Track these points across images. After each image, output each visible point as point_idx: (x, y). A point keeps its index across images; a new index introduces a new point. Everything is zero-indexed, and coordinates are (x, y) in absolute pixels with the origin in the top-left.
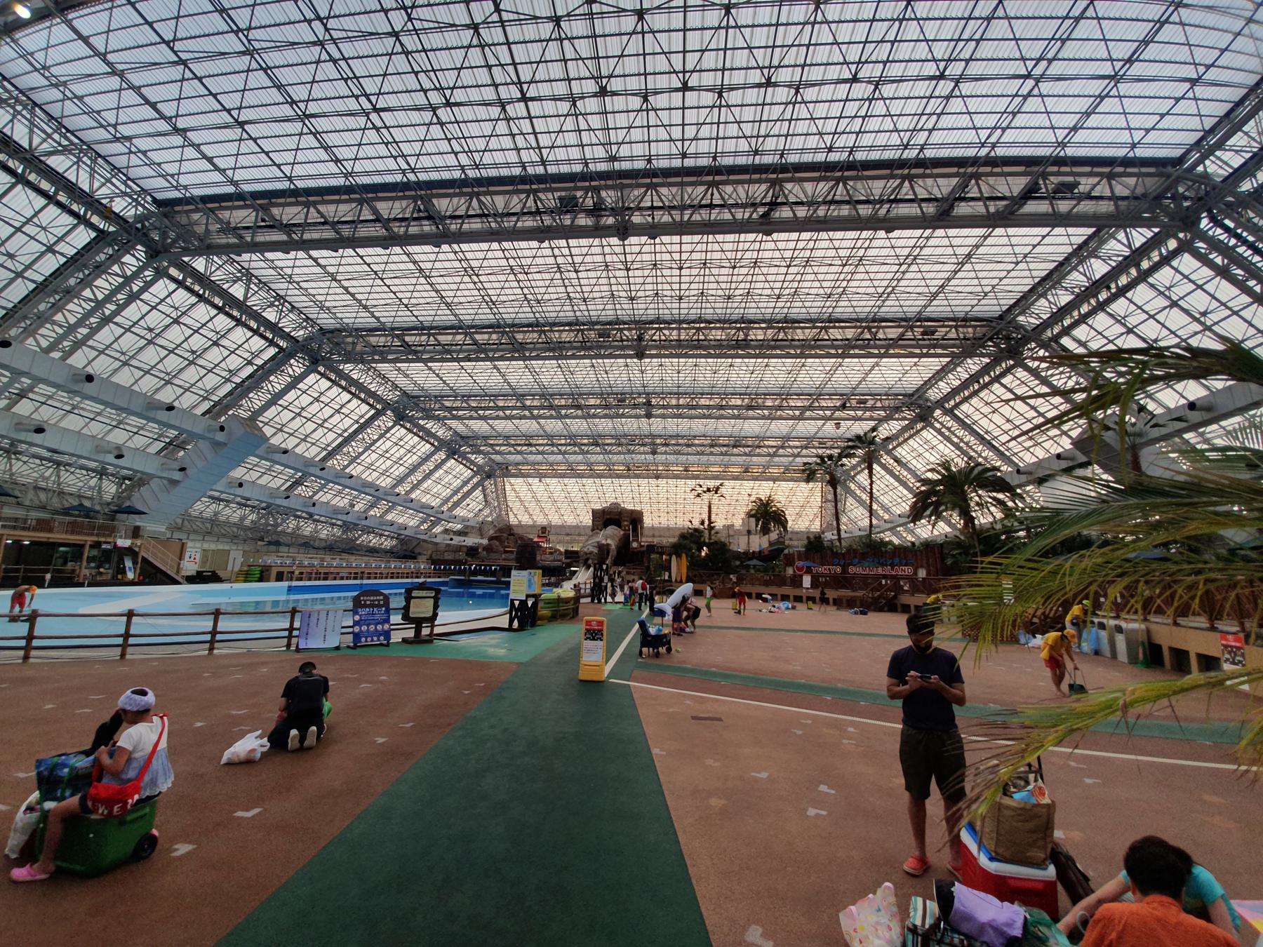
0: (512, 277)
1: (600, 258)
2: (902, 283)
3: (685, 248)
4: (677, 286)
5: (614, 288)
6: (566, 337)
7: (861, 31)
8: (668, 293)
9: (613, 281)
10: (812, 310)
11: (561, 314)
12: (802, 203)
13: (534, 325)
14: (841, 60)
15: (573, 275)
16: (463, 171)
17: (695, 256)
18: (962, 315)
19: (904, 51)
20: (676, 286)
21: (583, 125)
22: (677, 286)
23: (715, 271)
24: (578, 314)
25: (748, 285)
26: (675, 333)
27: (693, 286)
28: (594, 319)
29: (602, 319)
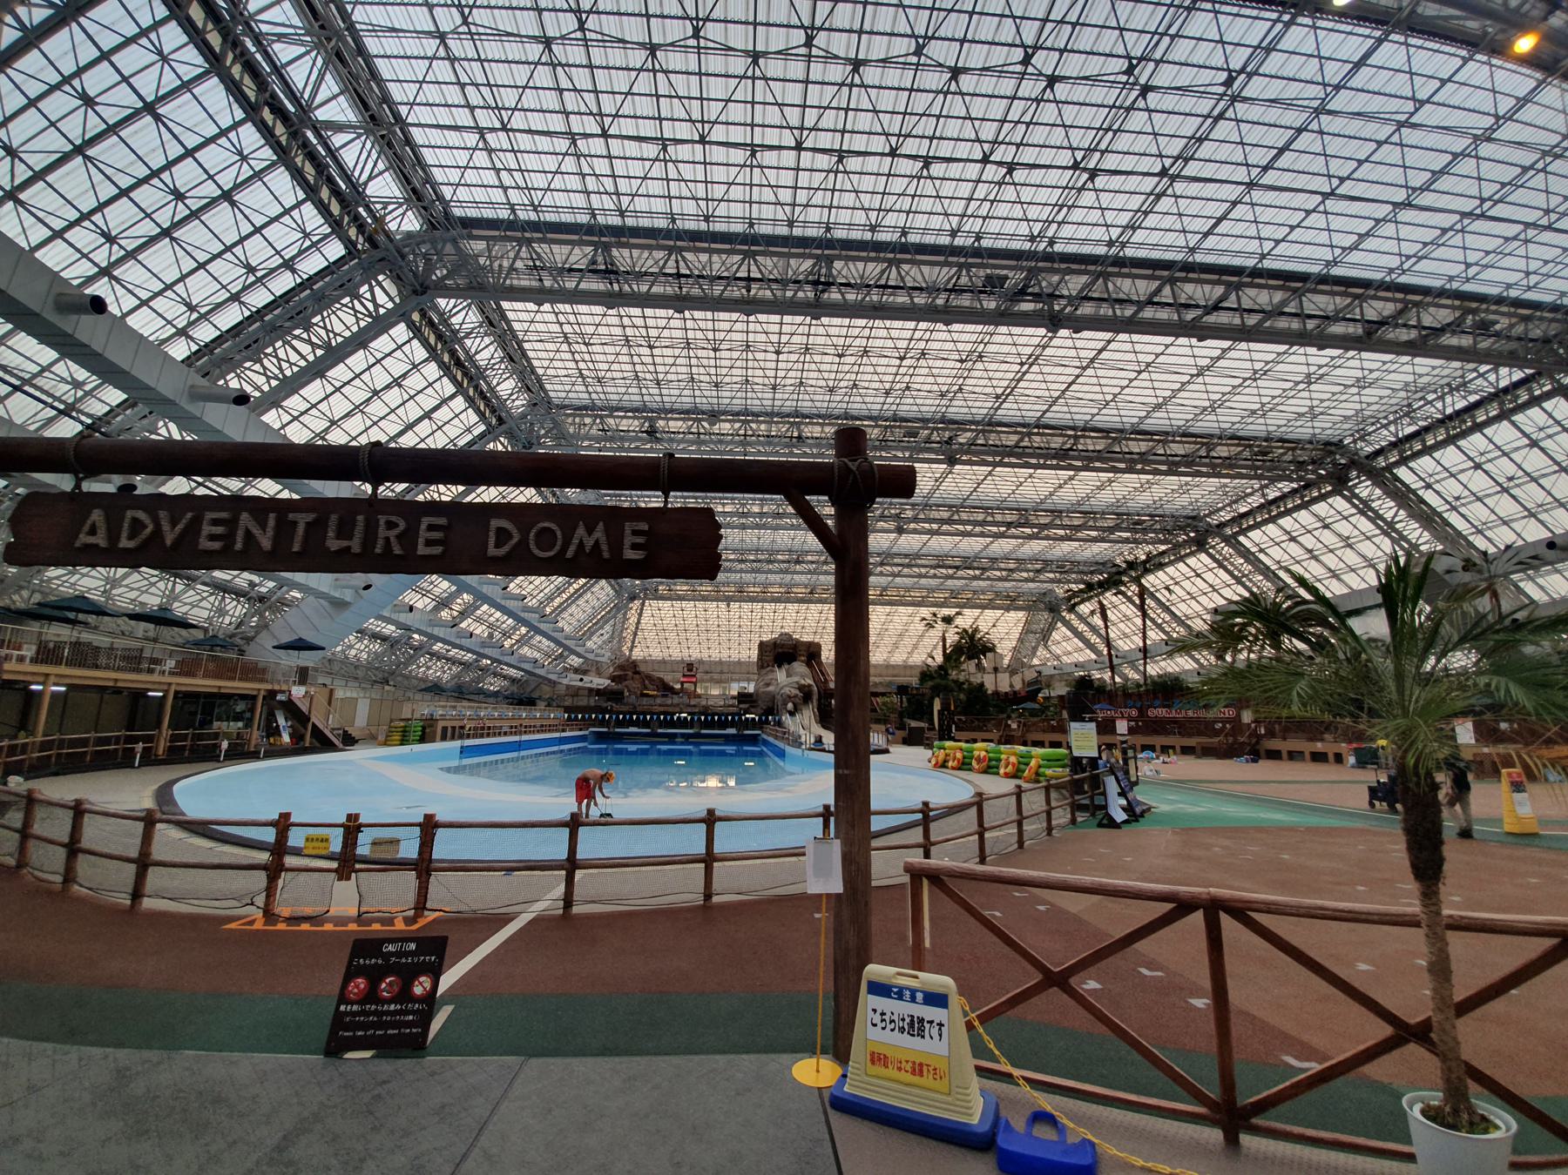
0: (565, 347)
1: (679, 334)
2: (1022, 384)
3: (786, 329)
4: (772, 373)
5: (695, 370)
6: (624, 425)
7: (997, 109)
8: (760, 380)
9: (694, 361)
10: (923, 409)
11: (626, 397)
12: (921, 289)
13: (589, 408)
14: (973, 136)
15: (647, 351)
16: (513, 211)
17: (795, 339)
18: (1081, 424)
19: (1038, 135)
20: (771, 373)
21: (673, 174)
22: (772, 373)
23: (817, 358)
24: (646, 398)
25: (853, 377)
26: (763, 427)
27: (791, 374)
28: (668, 406)
29: (676, 406)
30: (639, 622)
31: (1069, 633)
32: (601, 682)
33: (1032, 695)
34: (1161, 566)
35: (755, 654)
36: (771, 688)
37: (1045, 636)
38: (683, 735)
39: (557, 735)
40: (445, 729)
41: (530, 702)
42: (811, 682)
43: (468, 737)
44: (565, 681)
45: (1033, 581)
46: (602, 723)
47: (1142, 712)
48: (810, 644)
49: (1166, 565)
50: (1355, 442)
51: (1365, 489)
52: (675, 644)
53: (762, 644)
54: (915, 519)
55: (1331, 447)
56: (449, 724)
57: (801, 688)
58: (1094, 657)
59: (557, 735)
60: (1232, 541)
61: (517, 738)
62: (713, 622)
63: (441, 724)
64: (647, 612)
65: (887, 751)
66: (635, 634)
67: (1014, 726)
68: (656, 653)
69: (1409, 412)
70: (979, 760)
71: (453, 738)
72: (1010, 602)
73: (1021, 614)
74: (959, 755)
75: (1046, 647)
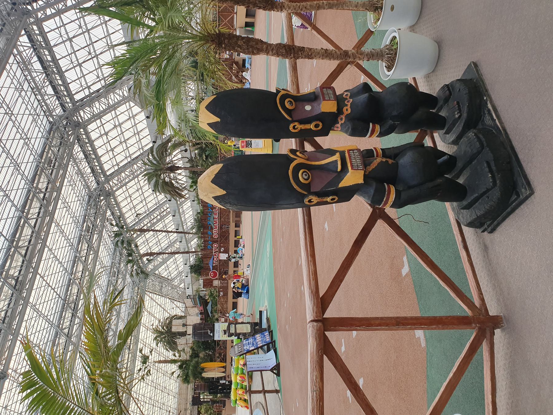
31: (163, 267)
33: (204, 302)
34: (122, 215)
47: (215, 241)
49: (120, 211)
50: (52, 116)
51: (85, 114)
55: (53, 127)
60: (108, 178)
69: (37, 90)
74: (240, 392)
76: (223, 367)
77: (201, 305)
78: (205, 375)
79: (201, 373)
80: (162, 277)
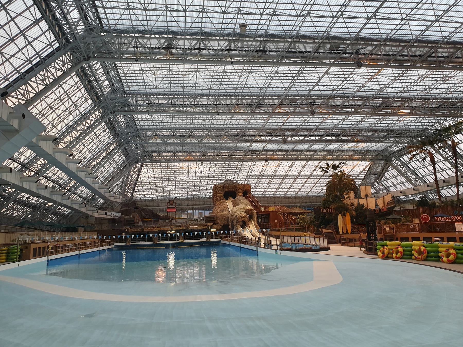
30: (139, 175)
32: (116, 215)
35: (210, 193)
36: (225, 213)
37: (380, 176)
38: (173, 244)
39: (98, 249)
40: (35, 249)
41: (75, 230)
42: (250, 207)
43: (52, 253)
44: (96, 215)
45: (382, 142)
46: (121, 240)
48: (244, 185)
52: (148, 190)
53: (215, 187)
54: (321, 106)
56: (37, 246)
57: (247, 211)
58: (410, 186)
59: (98, 249)
61: (77, 253)
62: (172, 175)
63: (33, 246)
64: (144, 171)
65: (328, 249)
66: (136, 184)
67: (388, 229)
68: (148, 195)
70: (419, 252)
71: (44, 255)
72: (362, 156)
73: (368, 163)
75: (380, 183)
76: (347, 232)
77: (387, 209)
78: (340, 217)
79: (340, 213)
80: (384, 174)
